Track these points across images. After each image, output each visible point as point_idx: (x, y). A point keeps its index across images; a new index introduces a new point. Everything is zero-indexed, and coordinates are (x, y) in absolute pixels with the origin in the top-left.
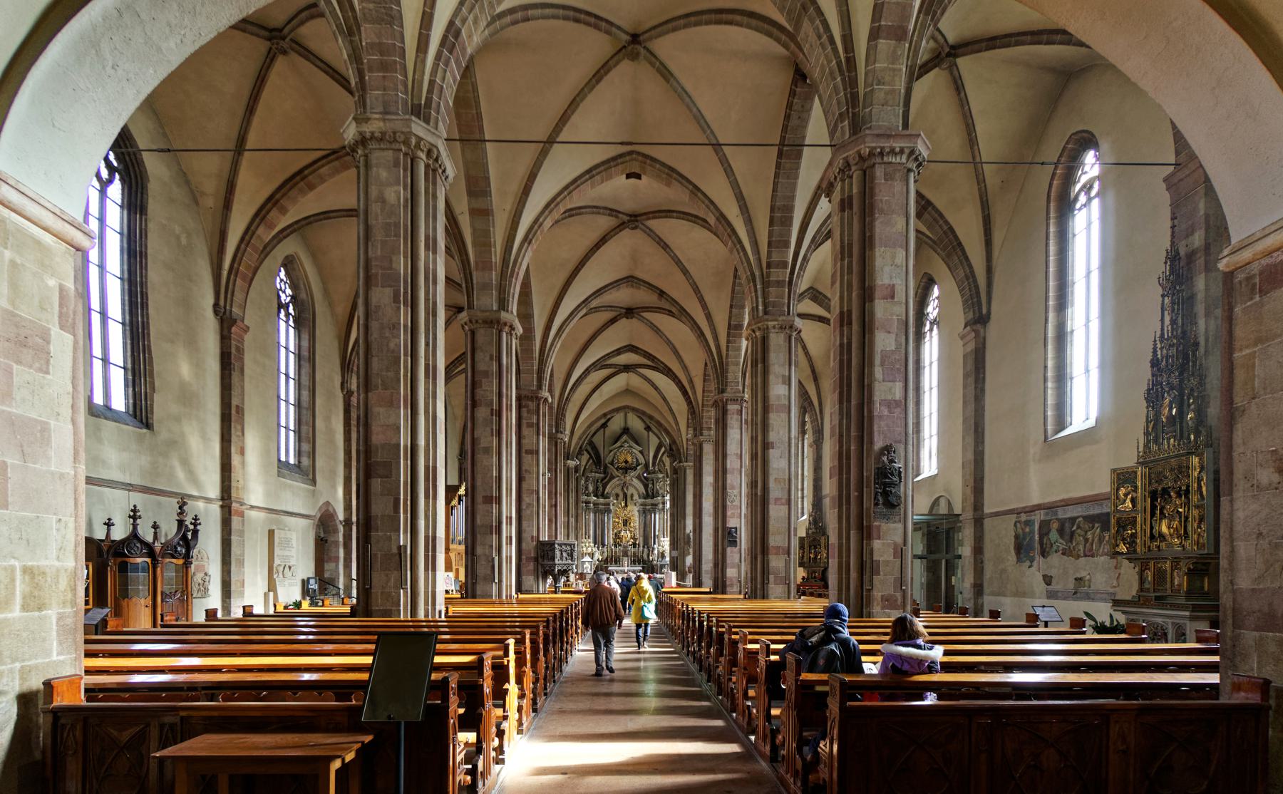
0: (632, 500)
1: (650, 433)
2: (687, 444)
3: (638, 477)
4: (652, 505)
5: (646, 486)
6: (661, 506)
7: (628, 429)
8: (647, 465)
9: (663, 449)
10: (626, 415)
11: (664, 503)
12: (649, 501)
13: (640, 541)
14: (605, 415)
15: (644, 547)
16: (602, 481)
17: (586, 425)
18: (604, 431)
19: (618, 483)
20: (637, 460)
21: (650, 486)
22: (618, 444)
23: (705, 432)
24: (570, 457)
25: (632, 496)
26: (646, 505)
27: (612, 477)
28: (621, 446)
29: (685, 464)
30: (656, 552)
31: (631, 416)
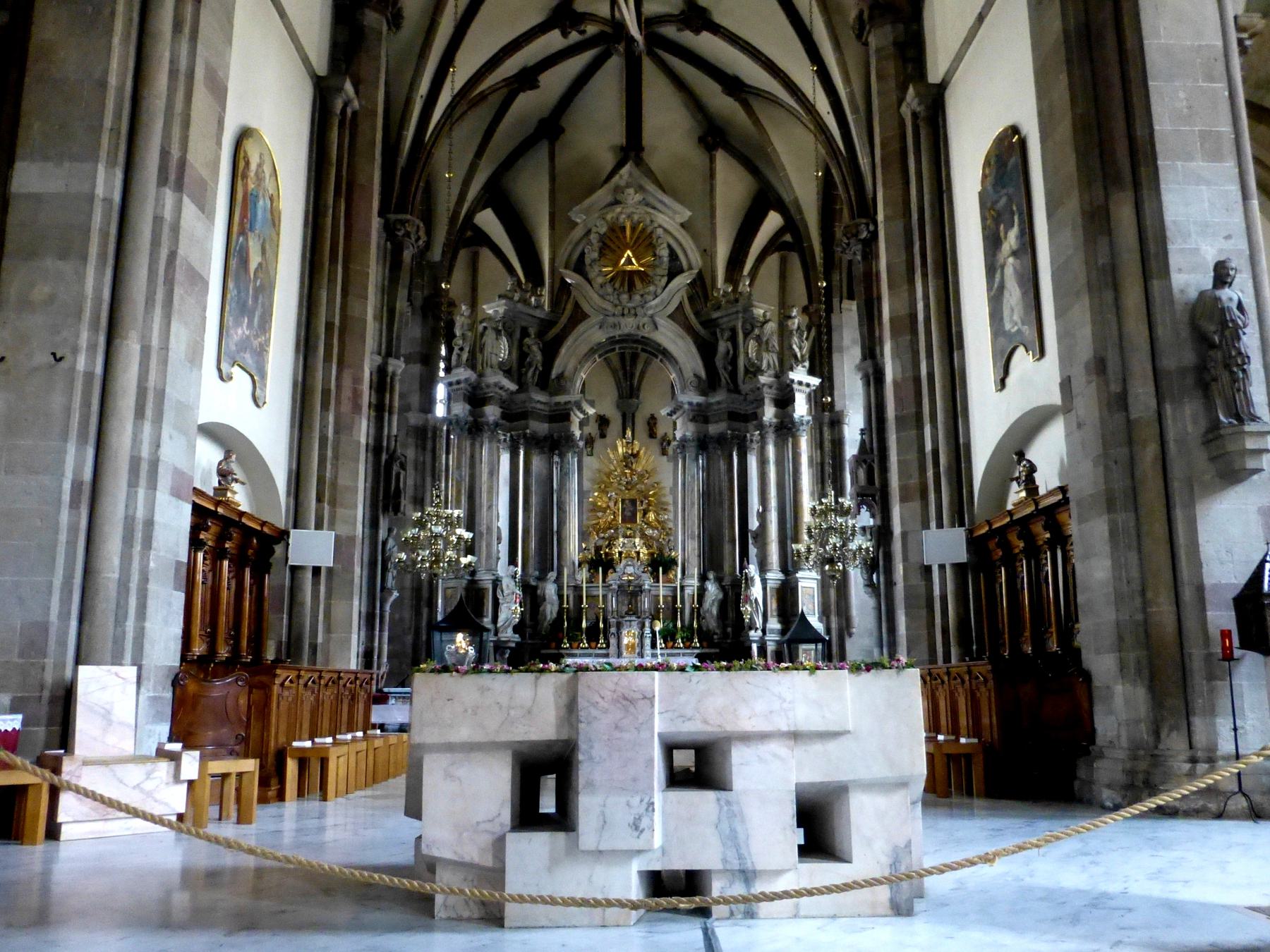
0: (652, 435)
1: (722, 159)
3: (677, 316)
4: (733, 416)
5: (706, 350)
6: (769, 413)
11: (785, 400)
12: (719, 397)
13: (687, 549)
15: (703, 578)
16: (540, 335)
19: (600, 336)
20: (673, 256)
21: (723, 346)
22: (602, 195)
25: (652, 422)
26: (706, 420)
27: (579, 316)
28: (617, 202)
30: (756, 591)
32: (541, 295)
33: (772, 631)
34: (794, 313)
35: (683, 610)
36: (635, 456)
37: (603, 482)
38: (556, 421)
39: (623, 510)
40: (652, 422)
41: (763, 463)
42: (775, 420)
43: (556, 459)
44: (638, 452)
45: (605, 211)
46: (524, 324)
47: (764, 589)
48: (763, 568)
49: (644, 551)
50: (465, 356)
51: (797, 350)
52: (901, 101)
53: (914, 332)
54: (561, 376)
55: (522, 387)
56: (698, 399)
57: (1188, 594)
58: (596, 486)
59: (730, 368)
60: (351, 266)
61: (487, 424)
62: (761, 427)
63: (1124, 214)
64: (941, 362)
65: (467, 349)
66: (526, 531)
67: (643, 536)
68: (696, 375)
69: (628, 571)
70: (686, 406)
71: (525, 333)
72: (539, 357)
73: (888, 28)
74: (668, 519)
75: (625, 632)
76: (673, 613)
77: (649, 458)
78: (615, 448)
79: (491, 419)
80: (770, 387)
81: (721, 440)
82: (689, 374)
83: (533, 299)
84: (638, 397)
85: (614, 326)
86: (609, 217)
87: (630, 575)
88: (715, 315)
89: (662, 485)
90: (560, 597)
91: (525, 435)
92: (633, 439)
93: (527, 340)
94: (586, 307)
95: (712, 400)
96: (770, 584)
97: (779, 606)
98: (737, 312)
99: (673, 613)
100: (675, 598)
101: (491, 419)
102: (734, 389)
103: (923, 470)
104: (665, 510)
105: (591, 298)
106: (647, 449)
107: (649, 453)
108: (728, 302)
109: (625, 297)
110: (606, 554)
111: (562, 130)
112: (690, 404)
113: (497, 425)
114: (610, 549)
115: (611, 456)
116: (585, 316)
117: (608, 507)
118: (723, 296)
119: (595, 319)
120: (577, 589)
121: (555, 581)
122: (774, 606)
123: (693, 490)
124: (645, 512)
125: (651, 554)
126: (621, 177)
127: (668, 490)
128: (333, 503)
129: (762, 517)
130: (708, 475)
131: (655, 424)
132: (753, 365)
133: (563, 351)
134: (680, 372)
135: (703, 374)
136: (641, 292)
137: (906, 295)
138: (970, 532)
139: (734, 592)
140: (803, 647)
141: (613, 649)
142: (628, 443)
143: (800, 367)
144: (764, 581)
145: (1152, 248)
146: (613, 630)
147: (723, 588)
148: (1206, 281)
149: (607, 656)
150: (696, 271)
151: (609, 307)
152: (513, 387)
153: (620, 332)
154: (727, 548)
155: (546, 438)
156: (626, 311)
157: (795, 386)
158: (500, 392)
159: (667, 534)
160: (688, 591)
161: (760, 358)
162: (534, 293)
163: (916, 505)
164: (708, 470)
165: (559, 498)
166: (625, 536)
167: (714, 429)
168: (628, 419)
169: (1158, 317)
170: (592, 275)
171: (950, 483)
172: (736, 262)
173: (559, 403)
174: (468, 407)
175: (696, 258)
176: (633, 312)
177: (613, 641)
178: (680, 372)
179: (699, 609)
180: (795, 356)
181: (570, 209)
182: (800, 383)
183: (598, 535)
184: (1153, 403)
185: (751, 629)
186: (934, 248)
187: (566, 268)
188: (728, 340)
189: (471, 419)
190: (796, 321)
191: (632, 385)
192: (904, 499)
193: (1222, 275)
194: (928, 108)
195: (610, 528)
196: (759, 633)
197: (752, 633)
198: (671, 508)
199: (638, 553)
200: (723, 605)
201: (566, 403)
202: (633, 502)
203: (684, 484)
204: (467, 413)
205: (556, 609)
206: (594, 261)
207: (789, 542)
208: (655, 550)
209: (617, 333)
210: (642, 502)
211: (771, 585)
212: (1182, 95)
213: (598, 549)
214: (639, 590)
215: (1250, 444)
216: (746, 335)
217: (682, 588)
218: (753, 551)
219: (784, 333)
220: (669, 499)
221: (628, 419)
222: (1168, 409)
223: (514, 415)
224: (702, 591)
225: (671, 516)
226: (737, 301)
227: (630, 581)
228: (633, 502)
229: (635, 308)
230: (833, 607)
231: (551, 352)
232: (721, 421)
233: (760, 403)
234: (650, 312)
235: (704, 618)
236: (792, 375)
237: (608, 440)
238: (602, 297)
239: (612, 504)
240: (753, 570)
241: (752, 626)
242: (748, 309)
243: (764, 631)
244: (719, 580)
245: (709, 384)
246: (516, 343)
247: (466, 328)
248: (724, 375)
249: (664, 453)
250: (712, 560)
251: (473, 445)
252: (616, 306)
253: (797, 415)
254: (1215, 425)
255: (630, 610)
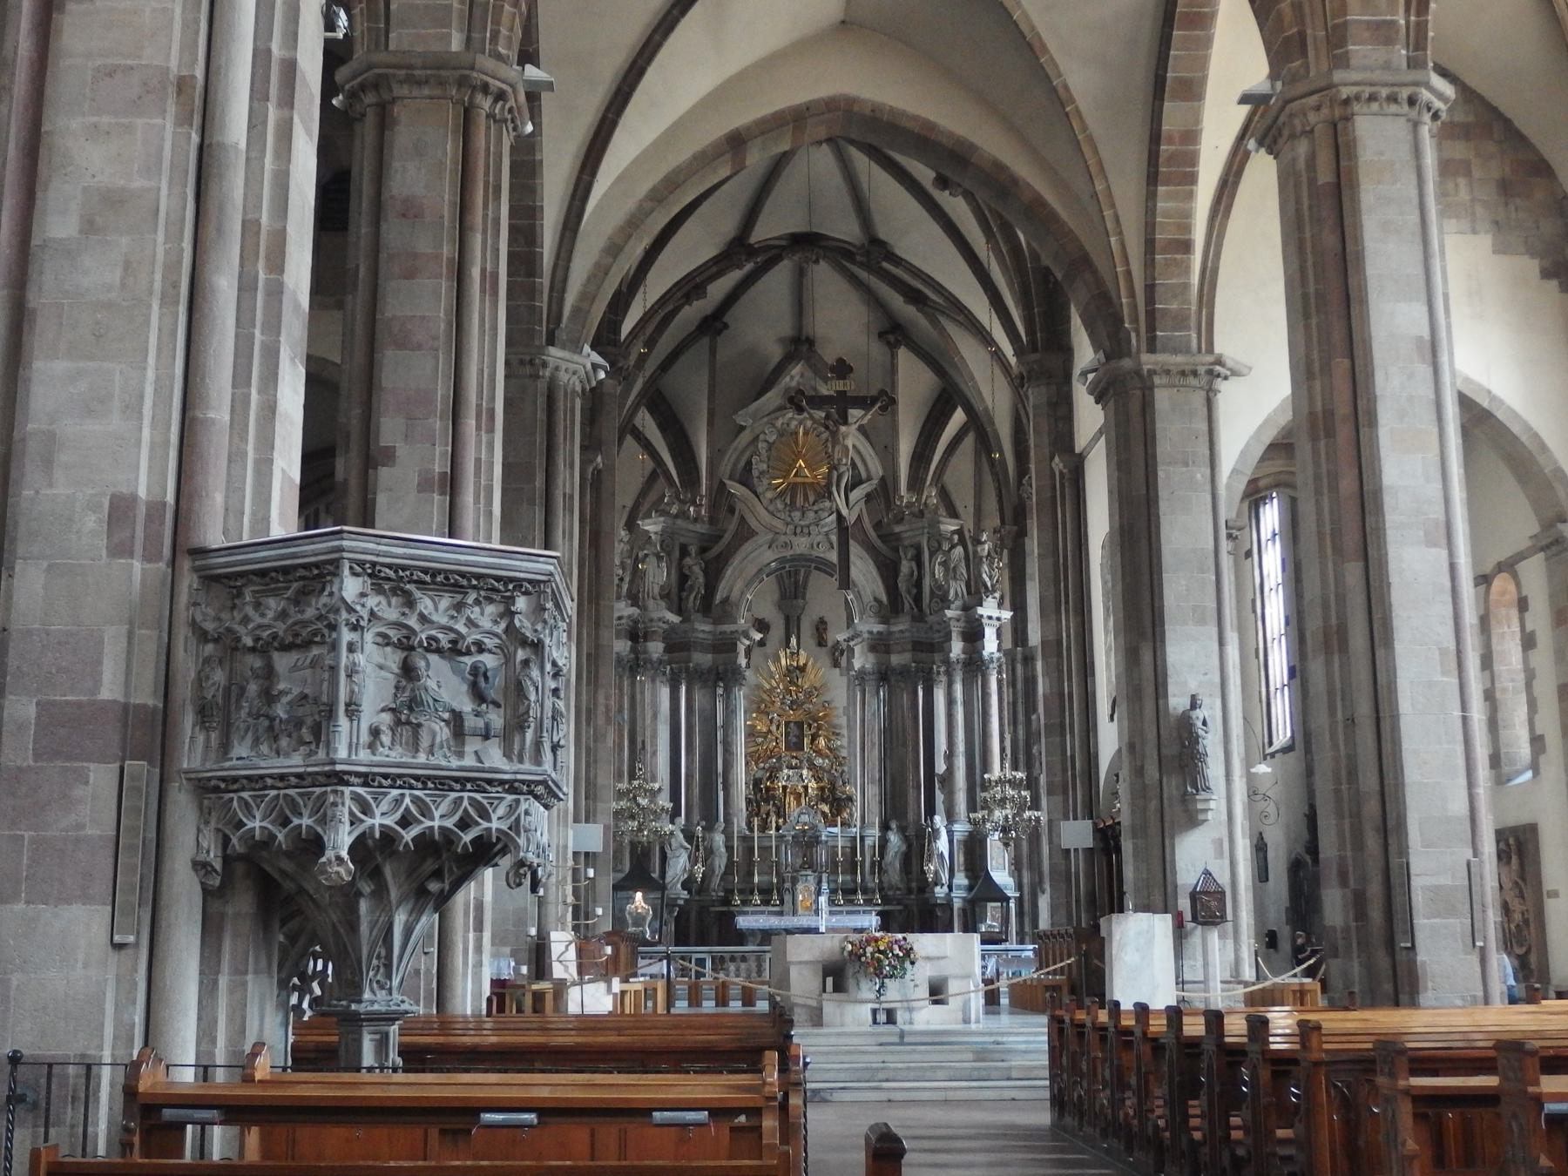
1: (903, 354)
2: (1150, 263)
5: (888, 570)
6: (957, 648)
7: (810, 342)
8: (886, 489)
9: (959, 417)
10: (800, 274)
11: (974, 635)
12: (901, 625)
13: (865, 795)
14: (736, 142)
15: (885, 827)
16: (703, 550)
17: (644, 187)
18: (713, 351)
19: (768, 556)
21: (906, 567)
23: (1361, 52)
24: (562, 335)
25: (821, 627)
26: (888, 651)
27: (745, 533)
29: (1148, 361)
30: (942, 844)
31: (824, 276)
32: (701, 505)
33: (959, 887)
34: (984, 538)
35: (863, 862)
36: (802, 669)
37: (763, 701)
38: (720, 652)
39: (787, 734)
40: (821, 627)
41: (950, 702)
42: (963, 656)
43: (720, 691)
44: (805, 665)
45: (773, 416)
46: (682, 540)
47: (951, 842)
48: (951, 817)
49: (813, 785)
50: (625, 587)
51: (987, 579)
52: (1052, 459)
53: (1060, 655)
54: (726, 601)
55: (686, 620)
56: (878, 628)
57: (1170, 889)
58: (755, 706)
59: (914, 591)
60: (602, 602)
61: (651, 661)
62: (947, 662)
63: (1147, 657)
64: (1079, 685)
65: (627, 579)
66: (689, 776)
67: (812, 766)
68: (876, 599)
69: (799, 817)
70: (866, 636)
71: (684, 552)
72: (701, 580)
73: (1043, 389)
74: (841, 746)
75: (800, 887)
76: (852, 866)
77: (820, 672)
78: (777, 659)
79: (655, 656)
80: (958, 620)
81: (904, 672)
82: (868, 598)
83: (692, 509)
84: (804, 598)
85: (785, 545)
86: (779, 423)
87: (805, 824)
88: (897, 529)
89: (833, 705)
90: (729, 848)
91: (687, 669)
92: (799, 648)
93: (688, 561)
94: (753, 523)
95: (894, 629)
96: (957, 837)
97: (966, 860)
98: (923, 528)
99: (852, 866)
100: (854, 848)
101: (655, 656)
102: (919, 617)
103: (1064, 770)
104: (838, 734)
105: (760, 512)
106: (815, 662)
107: (819, 665)
108: (912, 514)
109: (797, 515)
110: (768, 789)
111: (726, 326)
112: (870, 633)
113: (660, 662)
114: (772, 782)
115: (773, 669)
116: (752, 533)
117: (770, 731)
118: (907, 507)
119: (763, 538)
120: (746, 840)
121: (723, 832)
122: (962, 859)
123: (873, 729)
124: (814, 738)
125: (822, 789)
126: (792, 378)
127: (841, 710)
128: (595, 800)
129: (950, 756)
130: (890, 711)
131: (825, 629)
132: (940, 587)
133: (729, 572)
134: (859, 596)
135: (884, 599)
136: (815, 508)
137: (1053, 623)
138: (1095, 825)
139: (918, 845)
140: (990, 905)
141: (788, 906)
142: (792, 654)
143: (990, 599)
144: (950, 833)
145: (1160, 680)
146: (788, 885)
147: (906, 839)
148: (1186, 703)
149: (781, 913)
150: (875, 482)
151: (779, 524)
152: (674, 619)
153: (791, 552)
154: (911, 793)
155: (710, 670)
156: (799, 530)
157: (985, 621)
158: (665, 626)
159: (841, 764)
160: (868, 842)
161: (947, 582)
162: (693, 503)
163: (1059, 799)
164: (890, 703)
165: (726, 736)
166: (790, 767)
167: (896, 660)
168: (792, 625)
169: (1161, 721)
170: (760, 490)
171: (1082, 783)
172: (921, 456)
173: (725, 632)
174: (629, 643)
175: (876, 469)
176: (806, 531)
177: (788, 898)
178: (859, 596)
179: (880, 863)
180: (986, 587)
181: (736, 412)
182: (990, 618)
183: (756, 764)
184: (1157, 776)
185: (936, 884)
186: (1074, 593)
187: (731, 478)
188: (911, 560)
189: (632, 656)
190: (986, 547)
191: (796, 582)
192: (1050, 793)
193: (1194, 704)
194: (1070, 471)
195: (771, 757)
196: (945, 889)
197: (937, 889)
198: (844, 732)
199: (806, 788)
200: (907, 859)
201: (732, 632)
202: (800, 725)
203: (863, 721)
204: (628, 649)
205: (724, 862)
206: (762, 473)
207: (978, 790)
208: (825, 783)
209: (788, 553)
210: (810, 726)
211: (957, 837)
212: (1183, 582)
213: (757, 783)
214: (815, 840)
215: (1200, 806)
216: (932, 554)
217: (862, 838)
218: (940, 797)
219: (972, 561)
220: (843, 721)
221: (792, 625)
222: (1165, 779)
223: (677, 645)
224: (884, 842)
225: (845, 741)
226: (921, 514)
227: (804, 831)
228: (800, 725)
229: (808, 526)
230: (1025, 861)
231: (714, 572)
232: (905, 651)
233: (948, 638)
234: (826, 529)
235: (886, 872)
236: (980, 611)
237: (769, 649)
238: (772, 513)
239: (774, 728)
240: (939, 820)
241: (937, 882)
242: (935, 524)
243: (950, 888)
244: (902, 830)
245: (890, 609)
246: (674, 564)
247: (625, 555)
248: (908, 601)
249: (836, 664)
250: (894, 809)
251: (633, 684)
252: (788, 524)
253: (985, 653)
254: (1185, 793)
255: (804, 863)
